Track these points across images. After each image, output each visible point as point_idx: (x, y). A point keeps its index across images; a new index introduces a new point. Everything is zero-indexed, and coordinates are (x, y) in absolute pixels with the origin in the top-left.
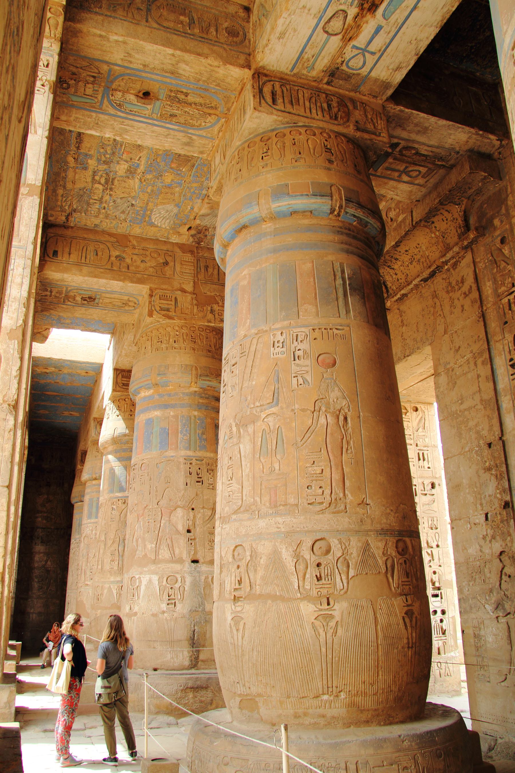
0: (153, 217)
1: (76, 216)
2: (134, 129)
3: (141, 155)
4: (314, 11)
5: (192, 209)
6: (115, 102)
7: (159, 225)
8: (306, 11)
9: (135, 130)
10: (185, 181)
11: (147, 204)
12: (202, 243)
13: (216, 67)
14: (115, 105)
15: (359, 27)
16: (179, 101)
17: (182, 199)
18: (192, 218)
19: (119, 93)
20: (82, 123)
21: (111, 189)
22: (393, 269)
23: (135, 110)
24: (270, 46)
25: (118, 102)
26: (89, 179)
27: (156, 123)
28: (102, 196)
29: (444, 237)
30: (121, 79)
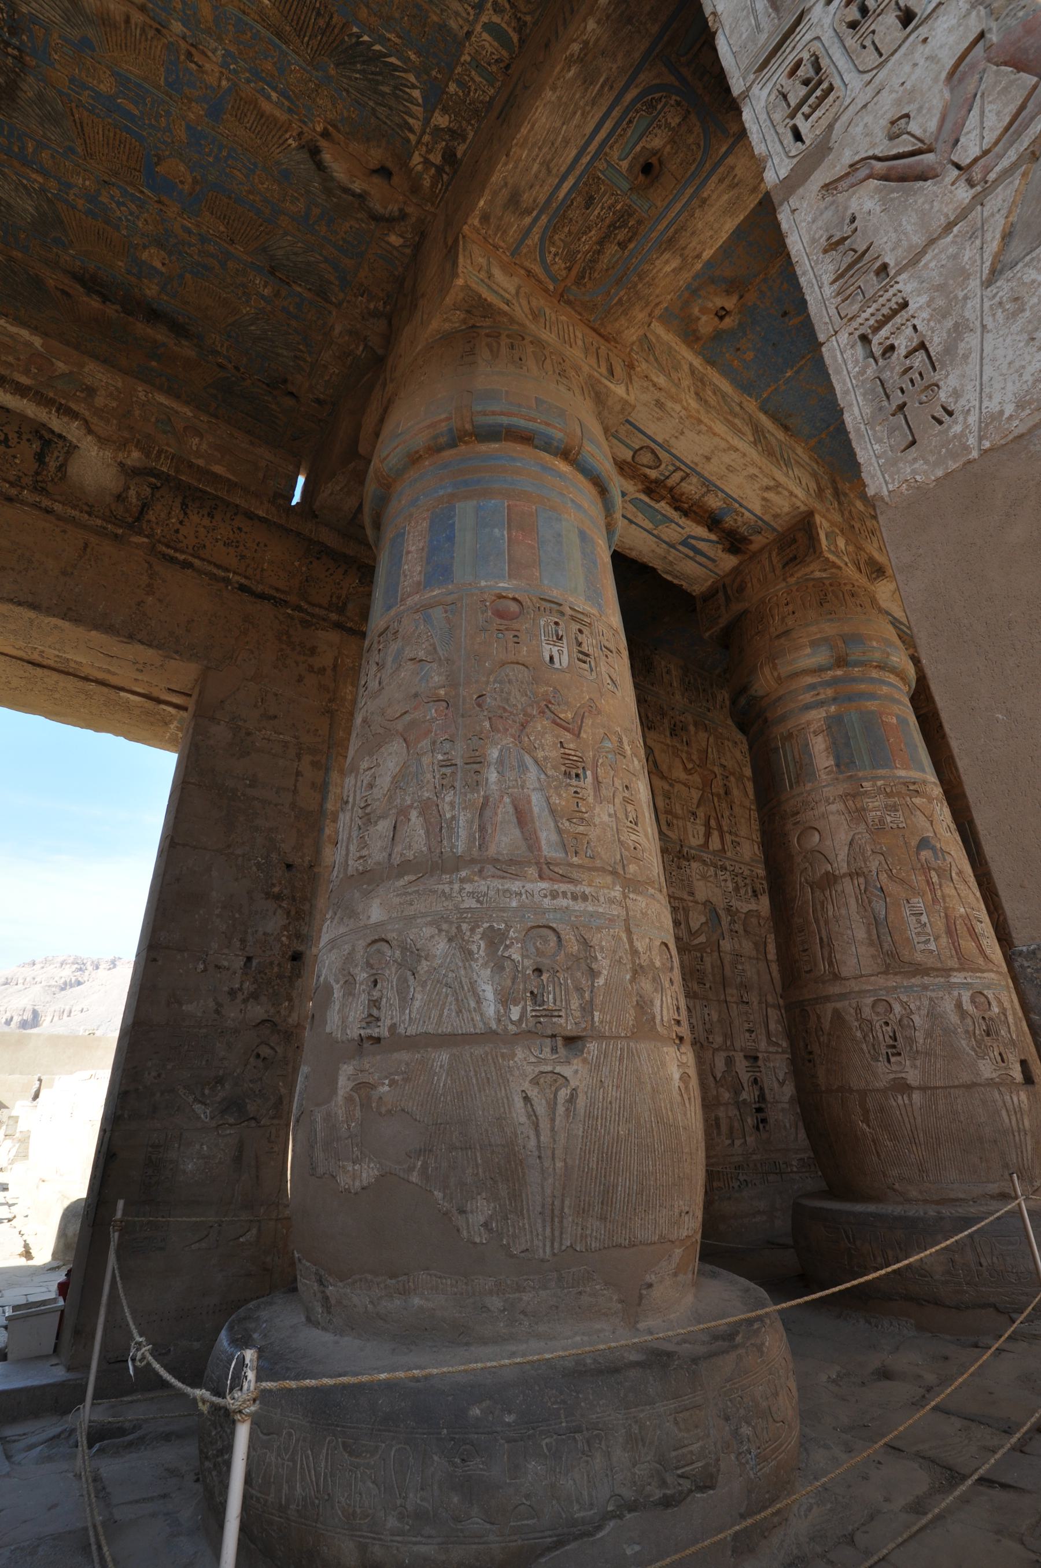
2: (586, 104)
4: (673, 441)
6: (664, 100)
8: (677, 434)
9: (581, 103)
13: (652, 311)
14: (657, 96)
15: (633, 478)
16: (613, 226)
19: (677, 120)
22: (186, 514)
23: (629, 132)
24: (652, 389)
27: (585, 160)
29: (307, 581)
30: (702, 143)
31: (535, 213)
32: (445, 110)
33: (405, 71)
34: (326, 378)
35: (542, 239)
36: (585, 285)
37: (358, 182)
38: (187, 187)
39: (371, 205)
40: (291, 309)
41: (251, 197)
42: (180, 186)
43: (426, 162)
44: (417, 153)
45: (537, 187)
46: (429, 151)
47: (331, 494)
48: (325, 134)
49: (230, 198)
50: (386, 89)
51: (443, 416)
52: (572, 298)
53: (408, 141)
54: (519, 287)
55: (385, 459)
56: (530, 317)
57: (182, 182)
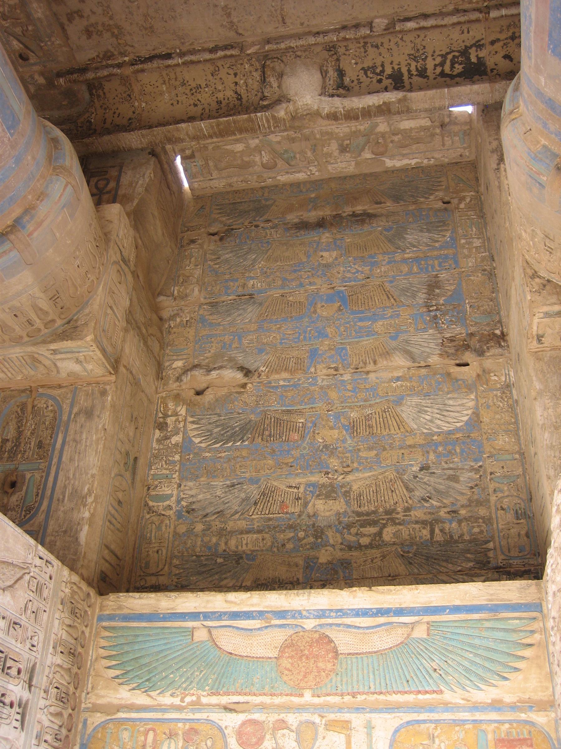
0: (446, 427)
1: (501, 557)
3: (283, 487)
5: (398, 379)
6: (23, 517)
7: (470, 412)
10: (328, 411)
11: (410, 446)
12: (498, 332)
16: (17, 445)
17: (378, 401)
18: (424, 371)
20: (66, 552)
21: (388, 512)
23: (35, 490)
25: (23, 513)
26: (375, 553)
28: (417, 522)
31: (73, 416)
32: (176, 445)
33: (209, 445)
34: (193, 259)
35: (61, 408)
36: (18, 406)
37: (215, 377)
38: (319, 306)
39: (201, 371)
40: (232, 284)
41: (278, 326)
42: (323, 304)
43: (176, 414)
44: (184, 414)
45: (78, 428)
46: (177, 420)
47: (144, 175)
48: (244, 386)
49: (291, 317)
50: (216, 430)
51: (35, 234)
52: (23, 394)
53: (192, 416)
54: (58, 372)
55: (66, 186)
56: (36, 356)
57: (323, 306)
